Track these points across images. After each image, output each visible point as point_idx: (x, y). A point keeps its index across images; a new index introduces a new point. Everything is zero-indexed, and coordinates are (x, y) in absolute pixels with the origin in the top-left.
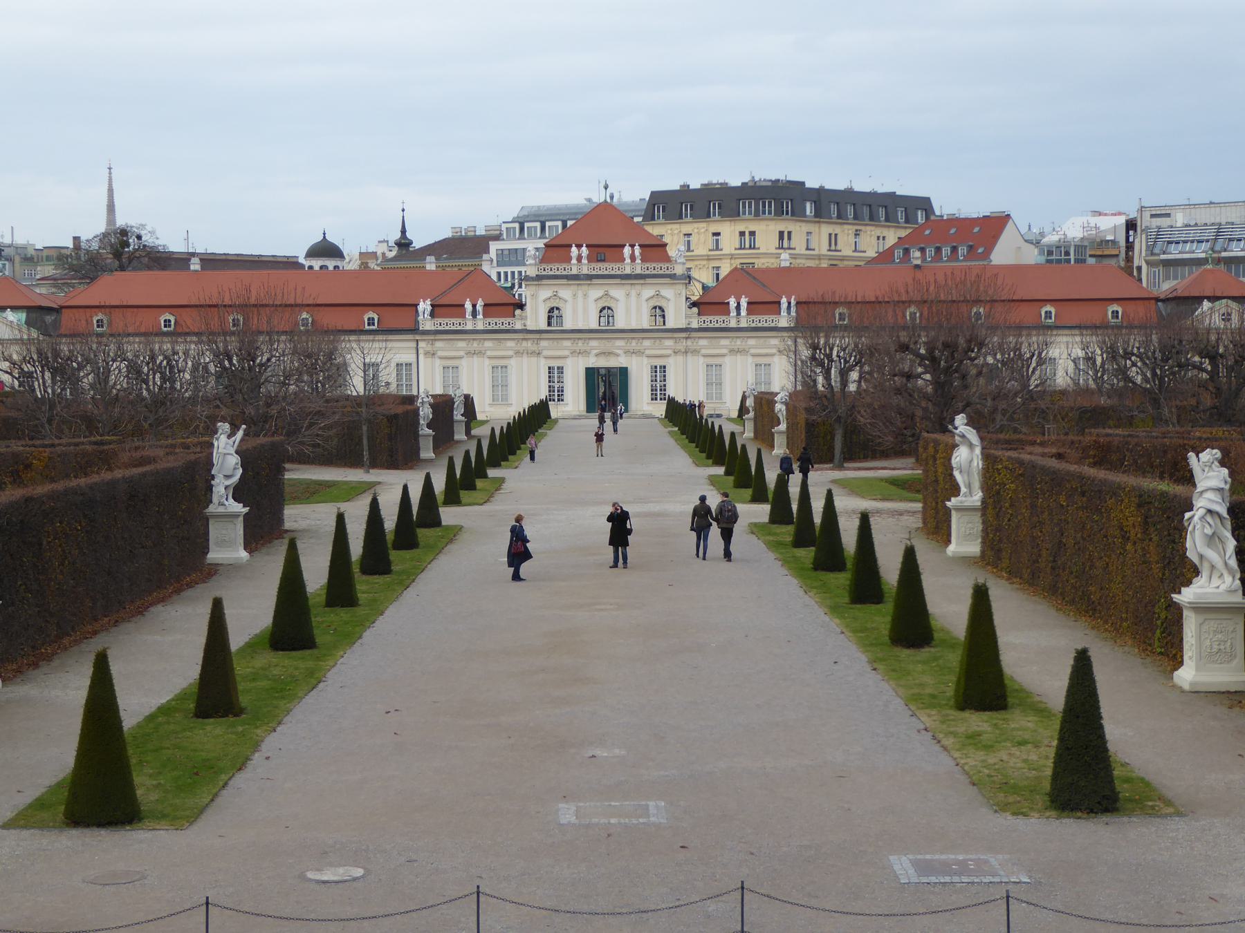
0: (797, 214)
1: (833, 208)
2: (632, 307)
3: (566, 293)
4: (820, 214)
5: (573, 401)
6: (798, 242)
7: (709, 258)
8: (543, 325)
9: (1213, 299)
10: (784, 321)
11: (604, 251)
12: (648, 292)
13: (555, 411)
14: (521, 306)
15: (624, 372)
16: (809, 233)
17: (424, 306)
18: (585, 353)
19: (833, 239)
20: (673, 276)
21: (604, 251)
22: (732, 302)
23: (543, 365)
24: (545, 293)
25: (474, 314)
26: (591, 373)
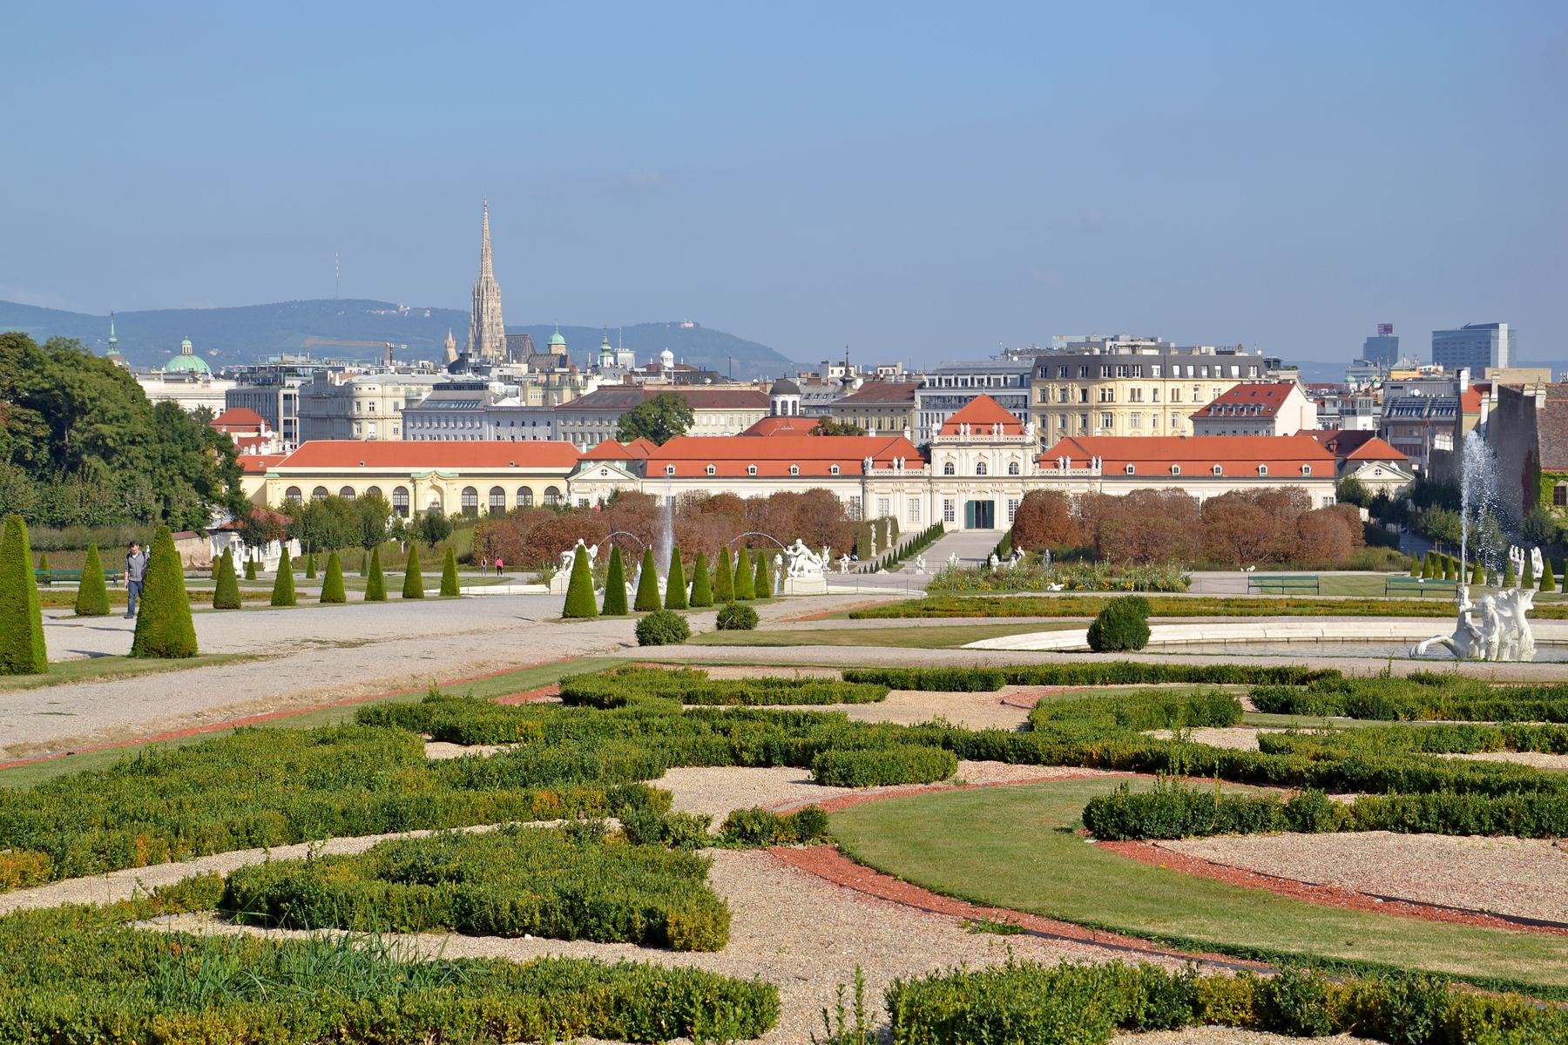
0: (1145, 374)
2: (998, 462)
4: (1166, 374)
5: (959, 522)
6: (1147, 396)
7: (1080, 408)
8: (941, 473)
9: (1370, 460)
12: (1006, 452)
13: (947, 527)
14: (929, 462)
15: (992, 503)
16: (1155, 391)
19: (1176, 395)
22: (1061, 460)
26: (969, 504)
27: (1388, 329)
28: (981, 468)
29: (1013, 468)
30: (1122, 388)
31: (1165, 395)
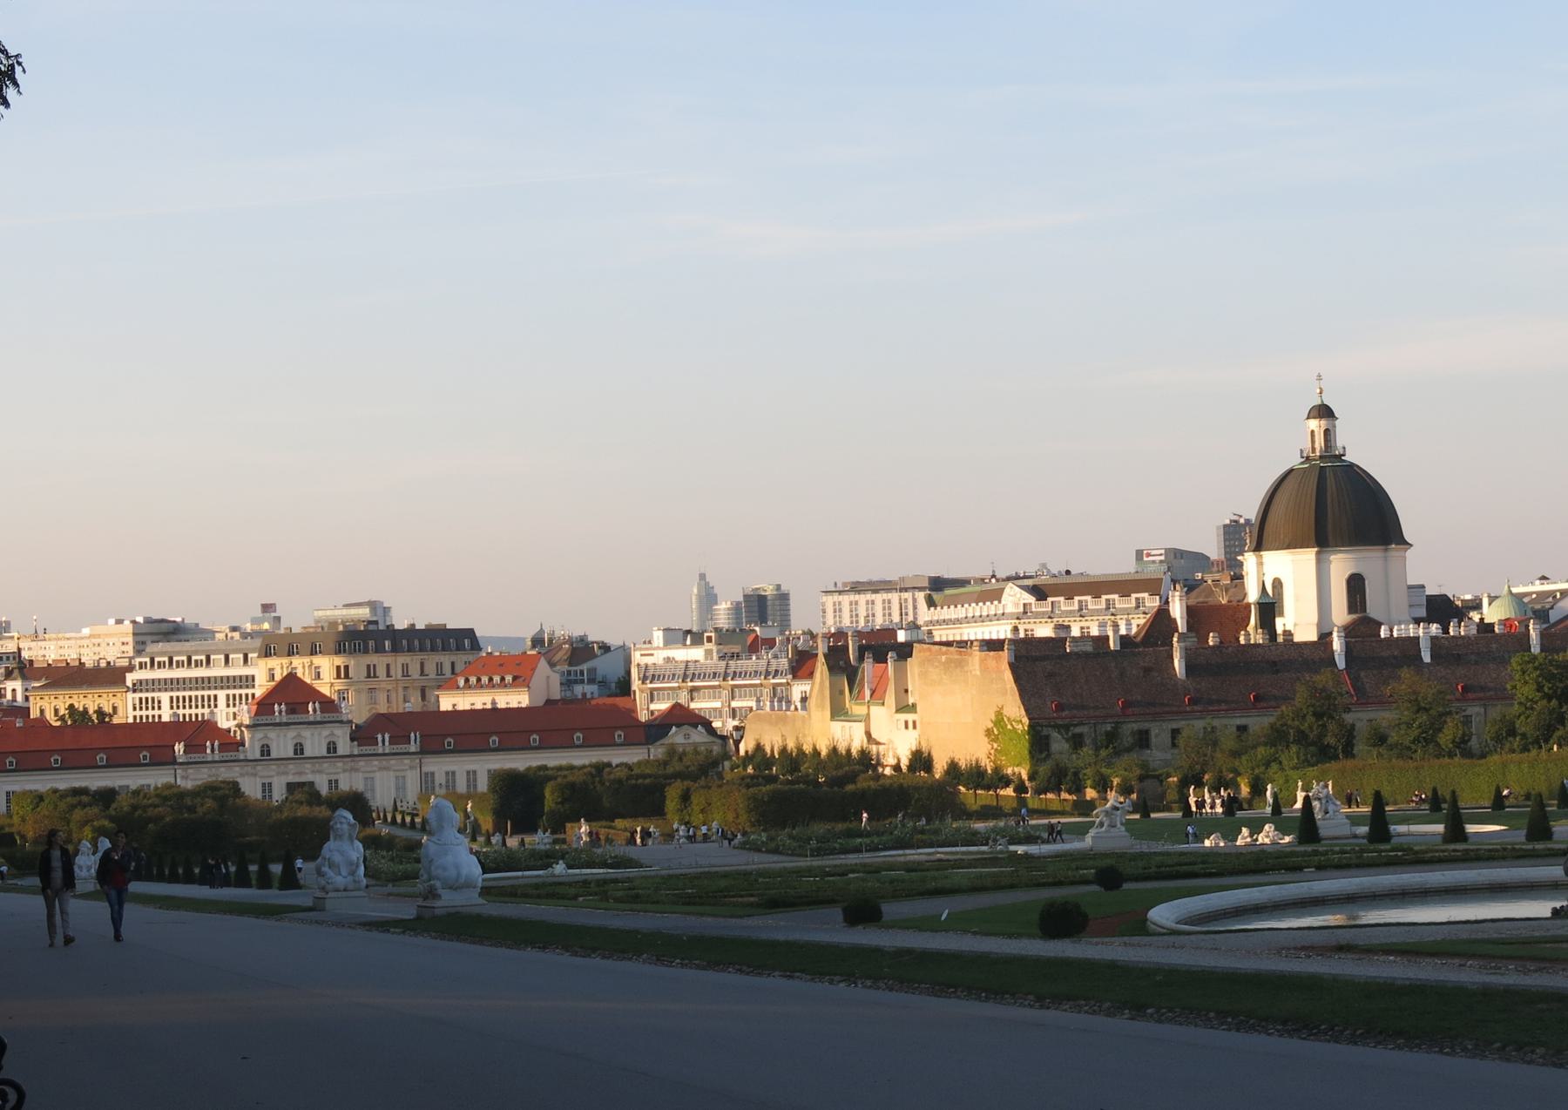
0: (379, 650)
1: (405, 642)
2: (315, 743)
3: (272, 734)
4: (396, 649)
6: (381, 672)
10: (413, 748)
11: (296, 708)
12: (326, 733)
17: (179, 748)
18: (286, 773)
19: (405, 667)
20: (341, 722)
21: (296, 708)
22: (380, 737)
23: (259, 782)
24: (259, 735)
25: (213, 750)
27: (267, 608)
28: (299, 749)
29: (332, 747)
30: (357, 665)
31: (397, 672)
